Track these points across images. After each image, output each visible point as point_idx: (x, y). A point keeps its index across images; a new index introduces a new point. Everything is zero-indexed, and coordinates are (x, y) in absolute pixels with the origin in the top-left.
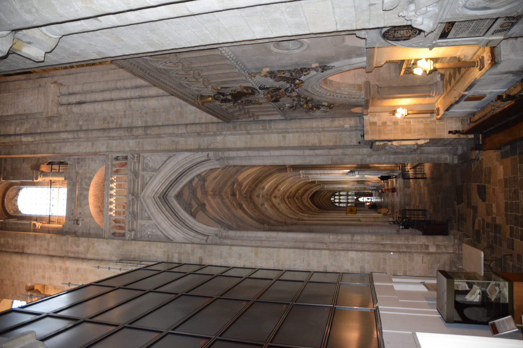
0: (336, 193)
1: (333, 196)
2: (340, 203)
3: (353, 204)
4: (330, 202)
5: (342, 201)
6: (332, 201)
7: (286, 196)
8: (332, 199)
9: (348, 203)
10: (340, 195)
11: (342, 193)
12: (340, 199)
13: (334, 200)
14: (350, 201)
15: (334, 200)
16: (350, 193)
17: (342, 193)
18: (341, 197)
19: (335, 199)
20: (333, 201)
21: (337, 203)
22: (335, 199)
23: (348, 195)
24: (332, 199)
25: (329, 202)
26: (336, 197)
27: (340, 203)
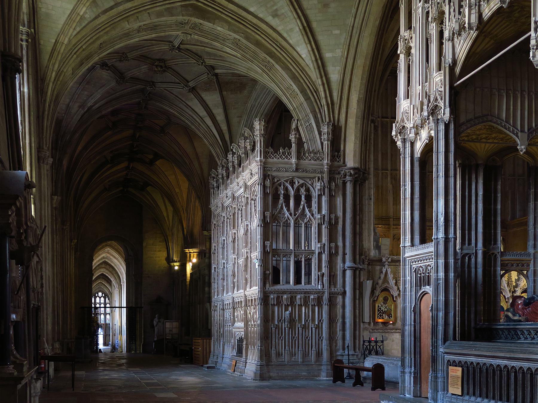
1: (103, 295)
6: (98, 295)
7: (107, 260)
8: (100, 294)
13: (98, 296)
15: (99, 297)
16: (108, 316)
19: (100, 298)
20: (97, 295)
21: (95, 300)
22: (100, 298)
24: (100, 294)
26: (102, 299)
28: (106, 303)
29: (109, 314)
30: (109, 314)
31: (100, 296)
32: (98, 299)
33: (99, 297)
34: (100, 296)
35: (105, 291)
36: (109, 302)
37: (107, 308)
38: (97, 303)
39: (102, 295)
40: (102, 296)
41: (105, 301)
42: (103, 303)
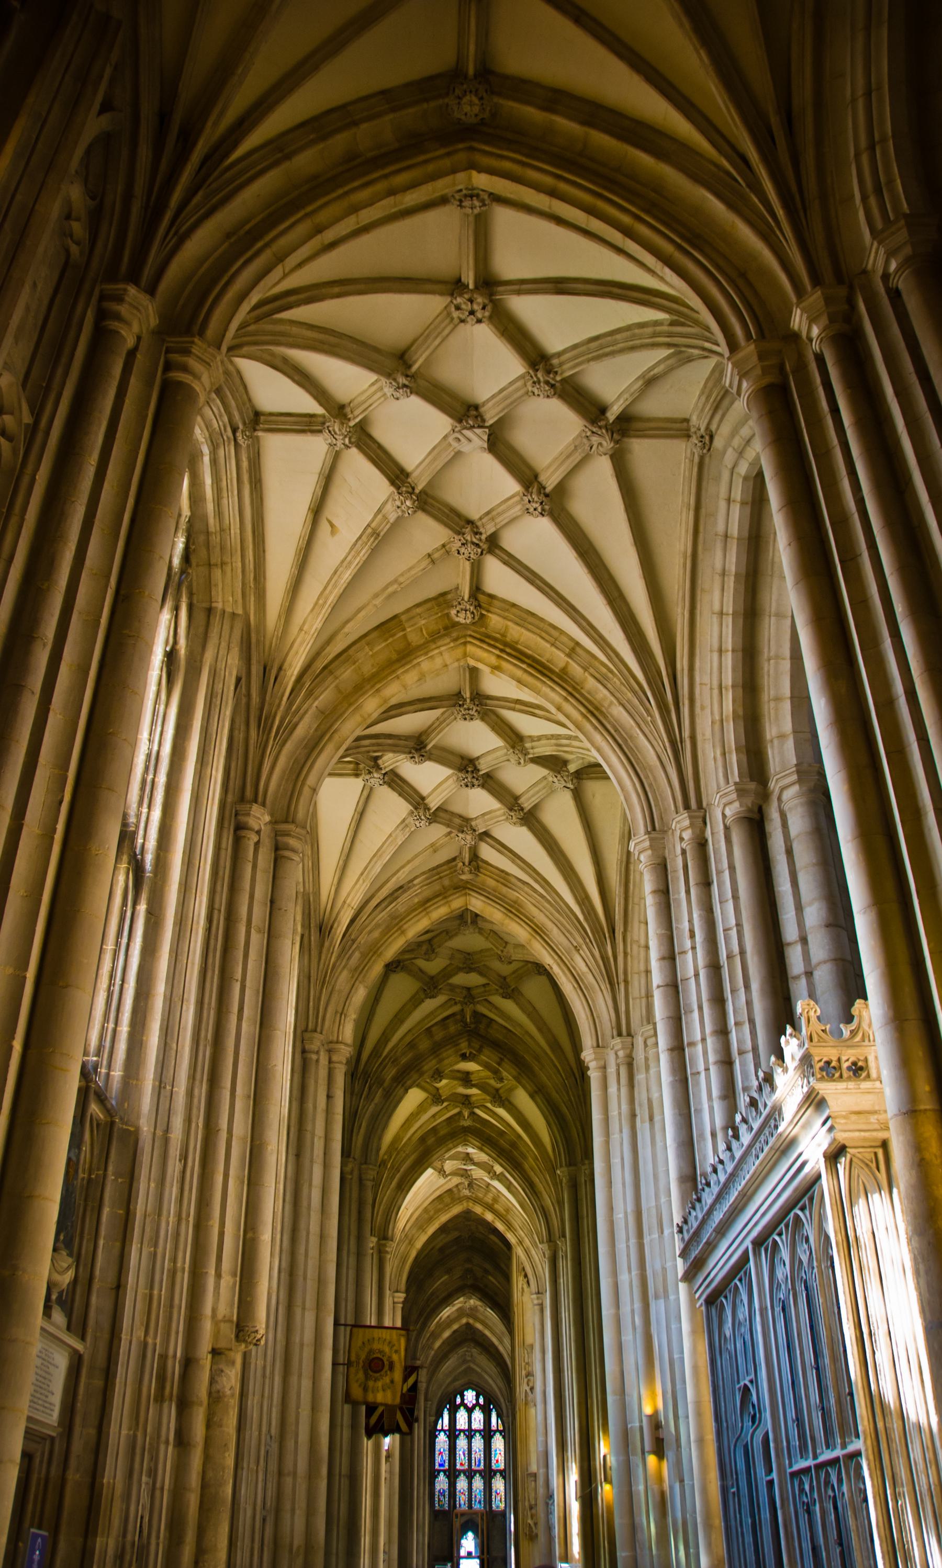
0: (498, 1416)
1: (481, 1401)
2: (453, 1434)
3: (444, 1503)
4: (458, 1384)
5: (462, 1443)
6: (463, 1399)
8: (470, 1396)
9: (452, 1474)
10: (487, 1434)
11: (498, 1443)
12: (470, 1434)
13: (463, 1403)
14: (462, 1484)
15: (466, 1406)
17: (498, 1443)
18: (478, 1443)
19: (470, 1411)
20: (458, 1400)
21: (453, 1421)
22: (470, 1411)
23: (488, 1474)
24: (470, 1396)
25: (455, 1380)
26: (478, 1415)
27: (453, 1434)
28: (490, 1430)
29: (503, 1473)
30: (503, 1473)
31: (470, 1405)
32: (462, 1416)
33: (466, 1406)
34: (470, 1405)
35: (486, 1382)
36: (501, 1428)
37: (473, 1427)
38: (461, 1431)
39: (477, 1399)
40: (477, 1404)
41: (487, 1421)
42: (479, 1431)
